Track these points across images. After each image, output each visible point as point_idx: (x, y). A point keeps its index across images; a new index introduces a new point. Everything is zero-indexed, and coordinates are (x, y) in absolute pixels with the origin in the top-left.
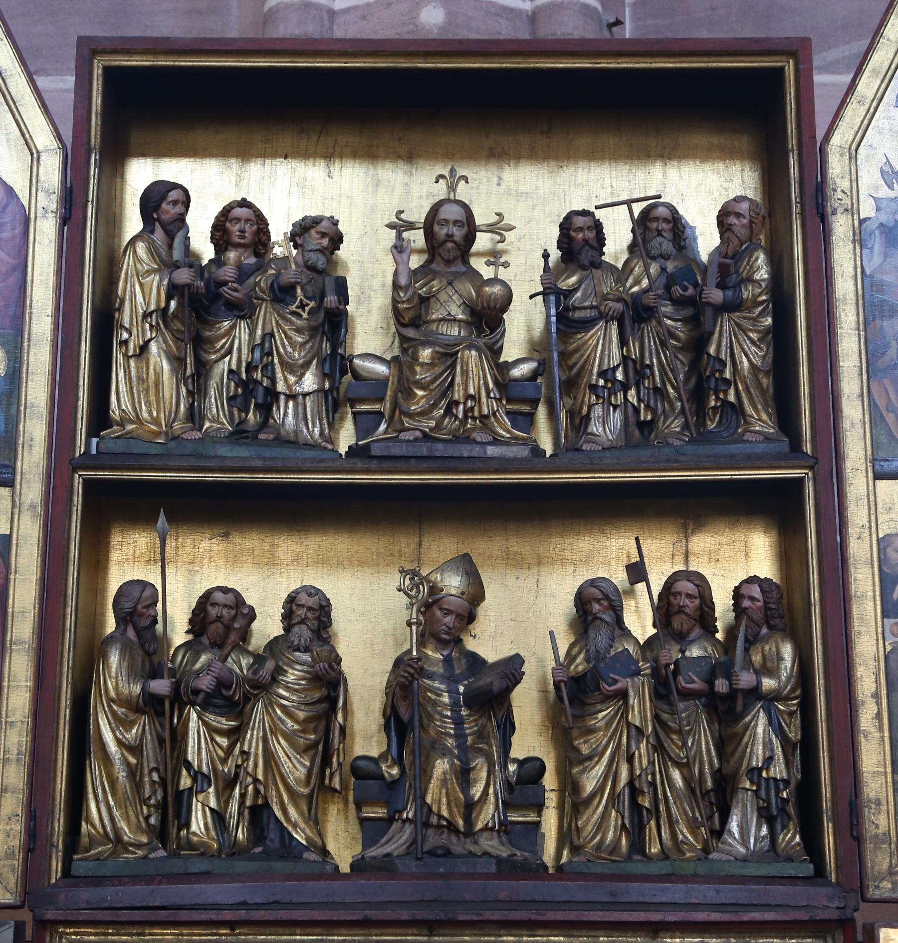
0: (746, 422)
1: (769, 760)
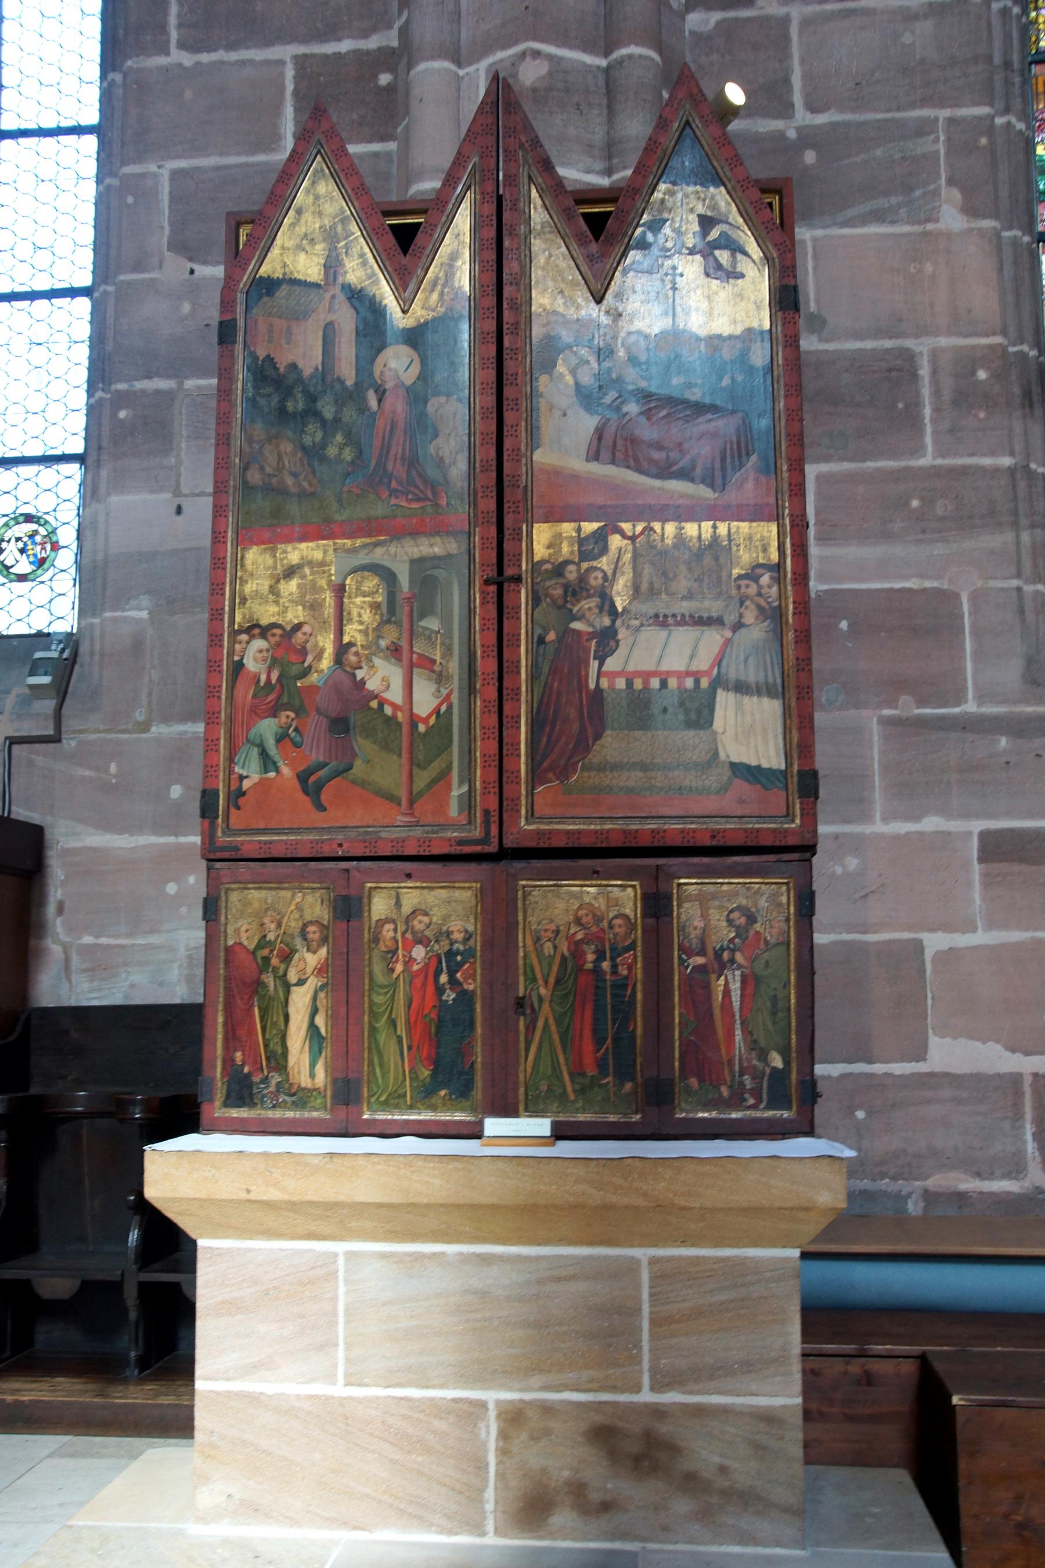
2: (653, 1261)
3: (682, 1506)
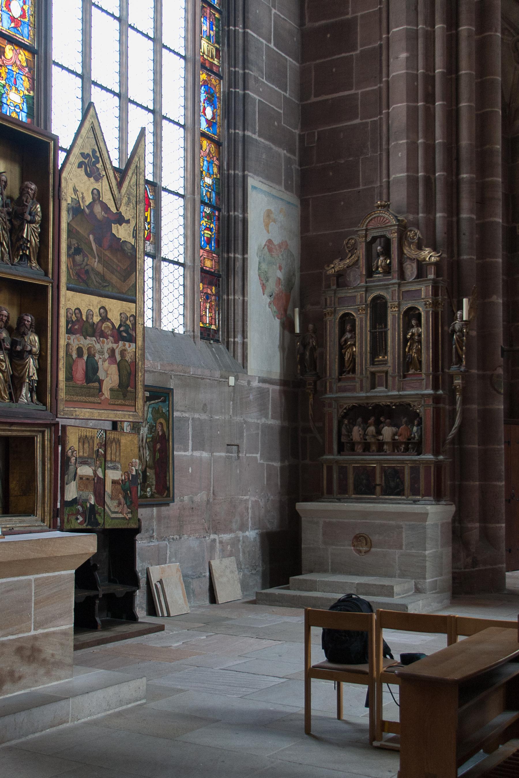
0: (30, 262)
1: (34, 374)
2: (36, 580)
3: (42, 671)
